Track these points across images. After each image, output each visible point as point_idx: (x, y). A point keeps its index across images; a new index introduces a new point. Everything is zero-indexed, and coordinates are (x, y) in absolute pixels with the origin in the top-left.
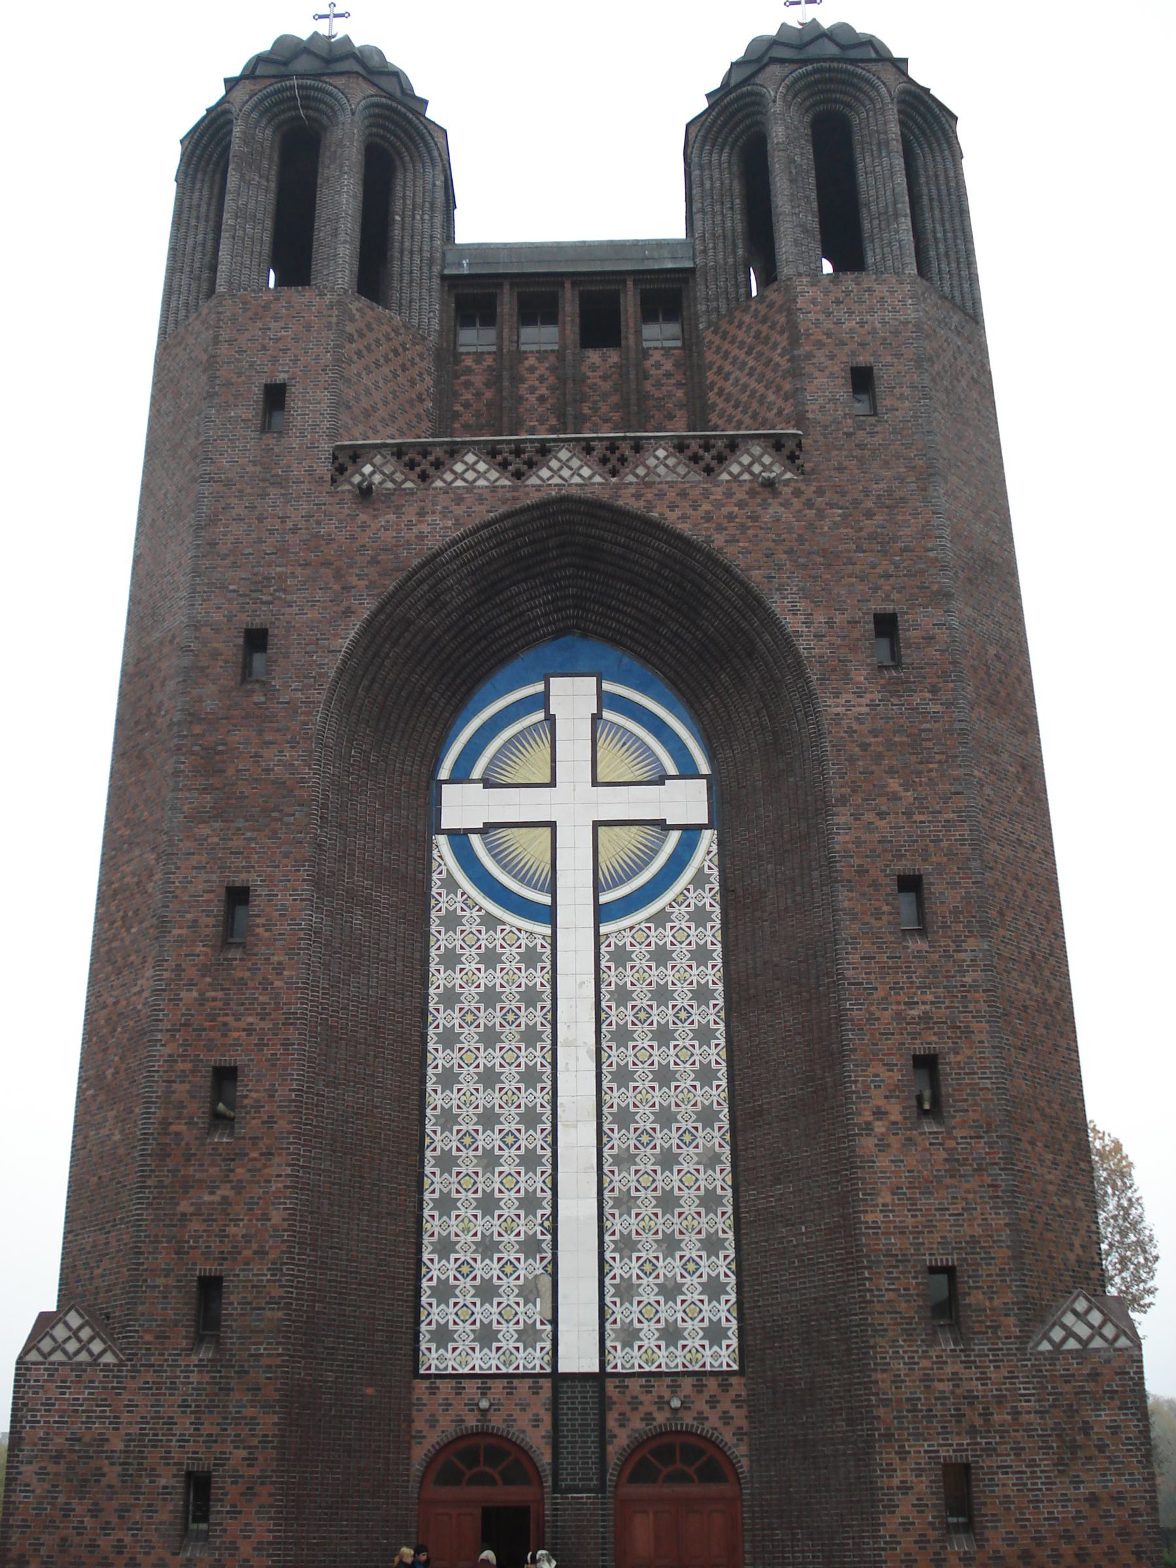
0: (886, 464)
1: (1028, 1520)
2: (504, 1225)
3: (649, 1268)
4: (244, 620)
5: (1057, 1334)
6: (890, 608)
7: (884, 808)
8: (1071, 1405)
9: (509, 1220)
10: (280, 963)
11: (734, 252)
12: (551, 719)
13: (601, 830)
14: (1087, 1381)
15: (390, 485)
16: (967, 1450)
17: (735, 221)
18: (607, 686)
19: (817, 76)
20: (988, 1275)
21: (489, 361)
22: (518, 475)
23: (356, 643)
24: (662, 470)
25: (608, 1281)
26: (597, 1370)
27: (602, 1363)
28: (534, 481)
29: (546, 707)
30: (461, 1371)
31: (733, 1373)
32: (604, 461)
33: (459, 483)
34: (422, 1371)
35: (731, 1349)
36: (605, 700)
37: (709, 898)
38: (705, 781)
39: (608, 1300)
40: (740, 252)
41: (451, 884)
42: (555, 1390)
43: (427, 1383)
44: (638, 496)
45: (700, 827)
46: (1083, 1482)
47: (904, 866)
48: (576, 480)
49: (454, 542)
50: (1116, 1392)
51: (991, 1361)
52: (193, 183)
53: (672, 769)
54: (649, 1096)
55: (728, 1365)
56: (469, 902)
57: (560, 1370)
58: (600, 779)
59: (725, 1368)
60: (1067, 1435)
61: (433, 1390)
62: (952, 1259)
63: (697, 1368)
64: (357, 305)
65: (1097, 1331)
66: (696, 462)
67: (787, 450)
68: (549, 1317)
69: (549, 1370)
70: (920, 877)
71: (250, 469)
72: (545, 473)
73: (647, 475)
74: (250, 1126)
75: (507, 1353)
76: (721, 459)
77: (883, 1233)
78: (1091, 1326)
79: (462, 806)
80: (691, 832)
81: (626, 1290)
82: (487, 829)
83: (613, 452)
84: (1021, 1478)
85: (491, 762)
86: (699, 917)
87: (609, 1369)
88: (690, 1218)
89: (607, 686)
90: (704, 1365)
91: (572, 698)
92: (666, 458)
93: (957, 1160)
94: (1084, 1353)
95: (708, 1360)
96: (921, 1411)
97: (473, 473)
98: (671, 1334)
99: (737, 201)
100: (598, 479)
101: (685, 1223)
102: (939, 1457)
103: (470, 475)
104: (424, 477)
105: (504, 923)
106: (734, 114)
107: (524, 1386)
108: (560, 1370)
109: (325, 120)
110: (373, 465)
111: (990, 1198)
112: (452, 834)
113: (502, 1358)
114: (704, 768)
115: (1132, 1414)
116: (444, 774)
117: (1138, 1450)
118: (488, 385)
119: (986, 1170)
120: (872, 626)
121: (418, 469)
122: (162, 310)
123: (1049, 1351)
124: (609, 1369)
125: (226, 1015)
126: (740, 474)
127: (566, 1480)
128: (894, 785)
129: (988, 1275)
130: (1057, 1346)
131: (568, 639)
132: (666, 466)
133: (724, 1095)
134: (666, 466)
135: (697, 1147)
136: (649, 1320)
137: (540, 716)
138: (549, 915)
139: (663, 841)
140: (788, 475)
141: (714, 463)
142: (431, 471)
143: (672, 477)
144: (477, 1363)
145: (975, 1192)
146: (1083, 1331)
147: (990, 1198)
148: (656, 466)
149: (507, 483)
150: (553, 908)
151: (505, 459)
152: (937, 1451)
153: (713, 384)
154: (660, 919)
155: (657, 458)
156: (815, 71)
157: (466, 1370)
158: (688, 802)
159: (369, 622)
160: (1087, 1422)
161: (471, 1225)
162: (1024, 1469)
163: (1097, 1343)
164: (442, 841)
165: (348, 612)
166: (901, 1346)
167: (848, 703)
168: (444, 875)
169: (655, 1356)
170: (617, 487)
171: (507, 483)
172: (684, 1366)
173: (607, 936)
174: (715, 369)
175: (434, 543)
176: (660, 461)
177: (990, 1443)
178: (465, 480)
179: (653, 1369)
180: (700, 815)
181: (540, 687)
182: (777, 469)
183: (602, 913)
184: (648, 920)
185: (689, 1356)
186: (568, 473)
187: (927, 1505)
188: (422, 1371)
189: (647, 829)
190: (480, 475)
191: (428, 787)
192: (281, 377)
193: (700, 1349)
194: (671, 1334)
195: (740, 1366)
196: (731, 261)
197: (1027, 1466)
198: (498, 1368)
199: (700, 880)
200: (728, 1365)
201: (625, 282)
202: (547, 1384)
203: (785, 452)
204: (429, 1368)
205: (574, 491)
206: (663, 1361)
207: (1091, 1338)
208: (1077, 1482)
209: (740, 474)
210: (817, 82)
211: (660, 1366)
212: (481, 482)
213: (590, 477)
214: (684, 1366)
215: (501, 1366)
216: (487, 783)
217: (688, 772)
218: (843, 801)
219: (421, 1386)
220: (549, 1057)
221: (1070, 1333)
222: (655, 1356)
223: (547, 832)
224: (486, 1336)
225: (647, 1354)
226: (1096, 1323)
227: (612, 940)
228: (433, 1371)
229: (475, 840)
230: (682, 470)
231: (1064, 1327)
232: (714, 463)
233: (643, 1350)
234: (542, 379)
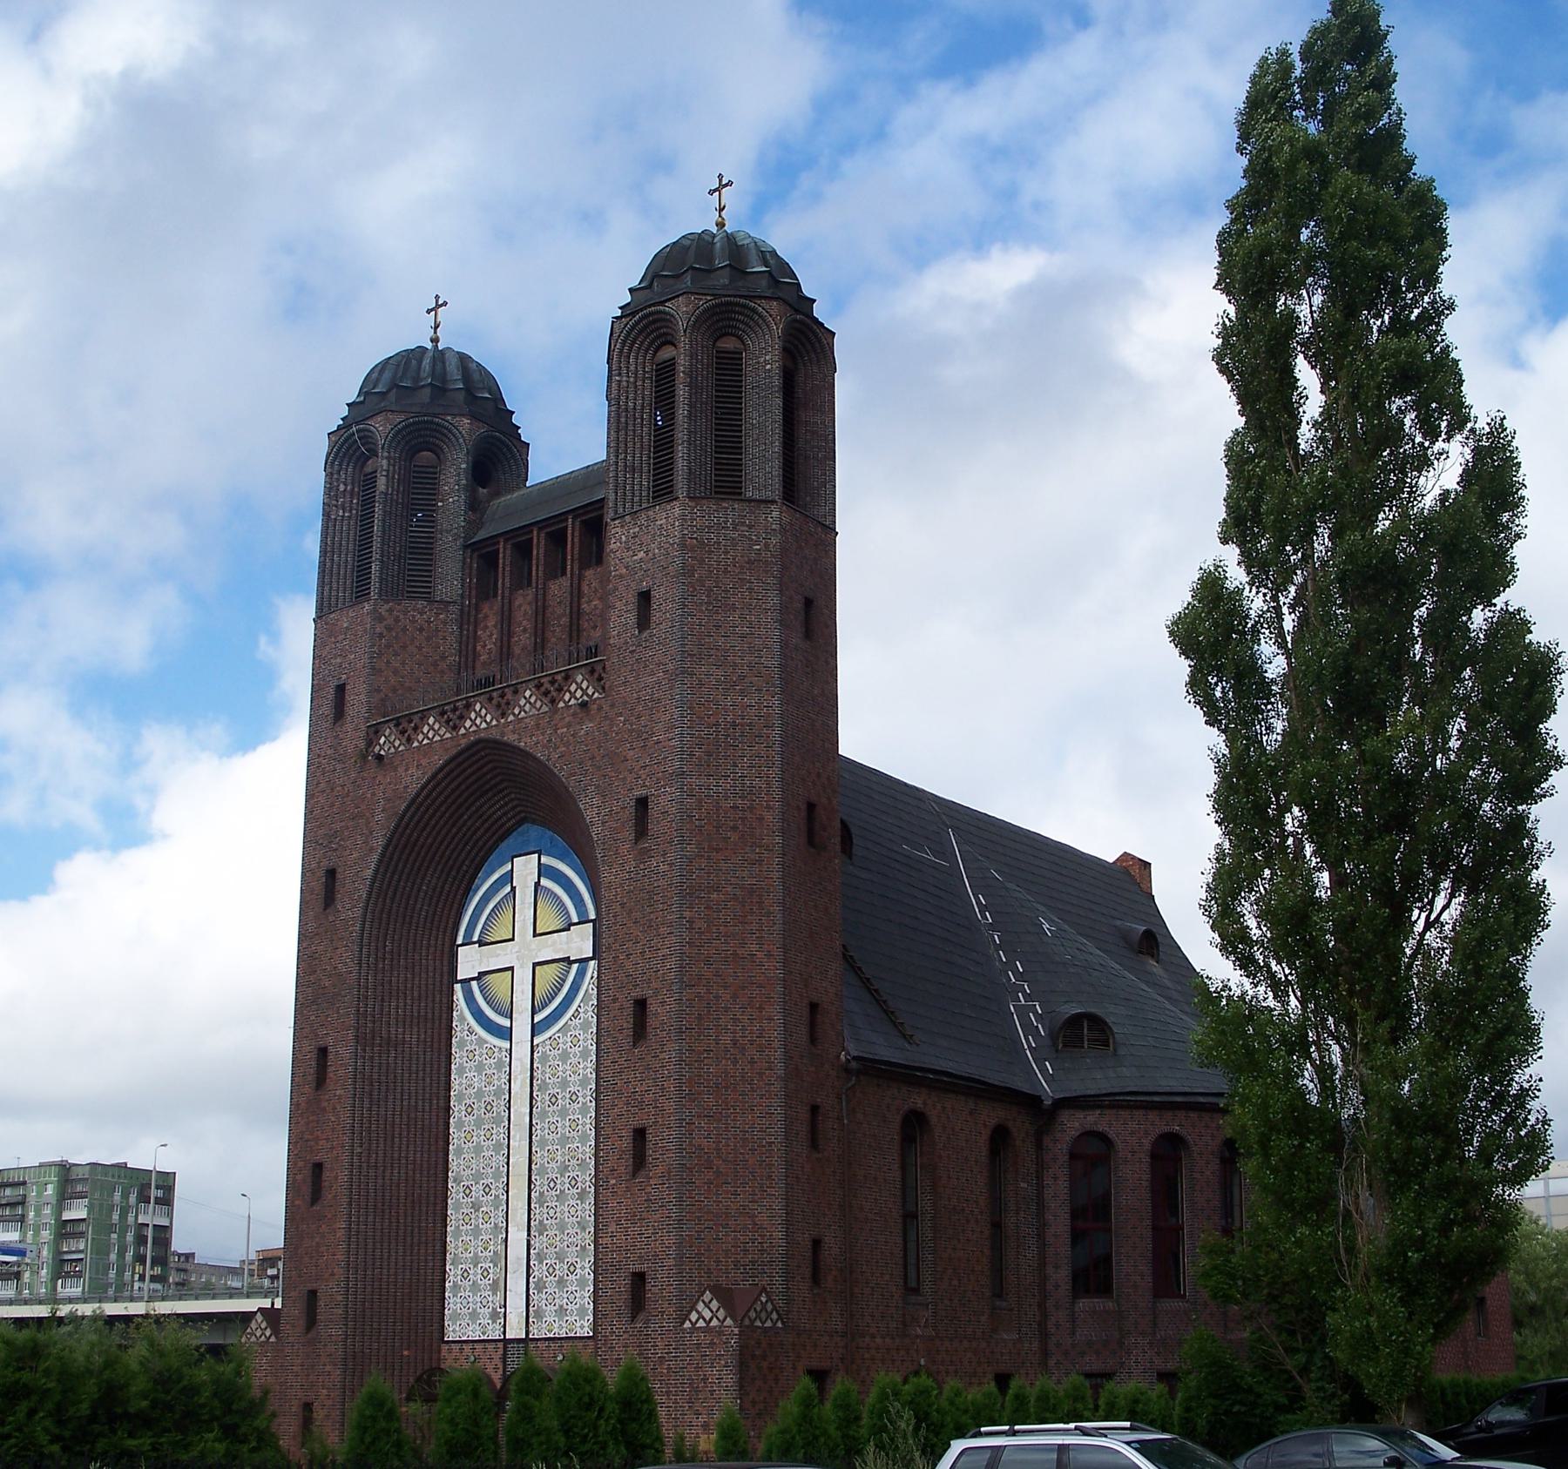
0: (652, 674)
3: (551, 1271)
5: (694, 1316)
12: (513, 889)
23: (377, 871)
27: (527, 1333)
28: (463, 731)
36: (543, 870)
41: (462, 1018)
42: (505, 1348)
44: (514, 732)
45: (587, 960)
48: (484, 725)
49: (423, 788)
61: (450, 1351)
65: (714, 1315)
67: (597, 674)
74: (328, 1196)
79: (469, 962)
81: (541, 1287)
82: (482, 974)
89: (543, 859)
91: (525, 869)
94: (708, 1329)
97: (433, 731)
98: (562, 1311)
107: (491, 1346)
116: (459, 941)
131: (525, 827)
138: (506, 1033)
146: (707, 1314)
156: (641, 320)
158: (580, 942)
159: (383, 855)
163: (715, 1322)
164: (458, 987)
165: (372, 849)
175: (414, 789)
176: (528, 703)
183: (535, 1030)
186: (480, 720)
189: (560, 965)
202: (500, 1345)
210: (646, 327)
219: (445, 1347)
221: (701, 1317)
225: (550, 1326)
230: (539, 704)
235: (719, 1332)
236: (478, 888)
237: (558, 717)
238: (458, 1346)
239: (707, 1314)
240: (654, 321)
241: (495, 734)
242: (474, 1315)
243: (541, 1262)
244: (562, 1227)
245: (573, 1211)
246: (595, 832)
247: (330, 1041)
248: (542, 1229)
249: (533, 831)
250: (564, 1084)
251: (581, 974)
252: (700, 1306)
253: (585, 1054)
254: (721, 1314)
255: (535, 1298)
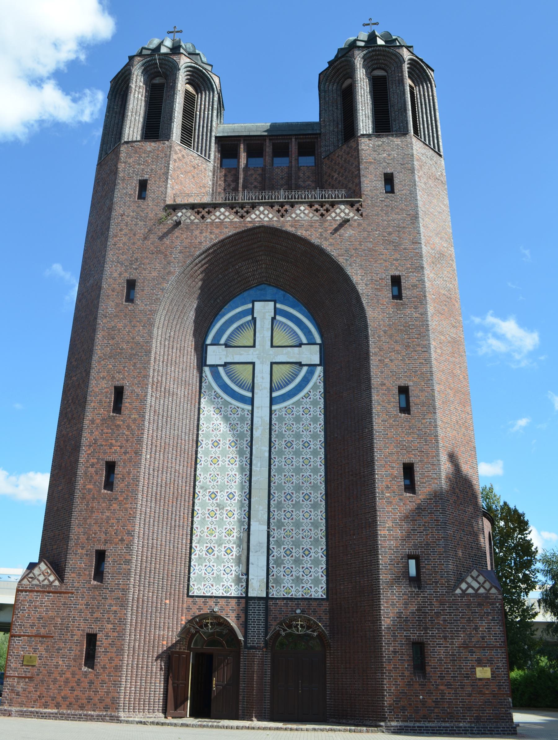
1: (450, 668)
2: (227, 532)
3: (288, 553)
4: (127, 276)
5: (464, 586)
6: (397, 273)
7: (393, 358)
8: (470, 618)
9: (230, 530)
10: (135, 418)
11: (338, 127)
12: (254, 319)
13: (274, 366)
14: (477, 607)
15: (189, 221)
16: (423, 636)
17: (338, 114)
18: (278, 306)
19: (374, 53)
20: (434, 559)
21: (233, 172)
22: (242, 217)
24: (302, 215)
25: (271, 557)
26: (264, 595)
27: (267, 593)
28: (249, 219)
29: (253, 314)
30: (207, 595)
31: (323, 599)
32: (279, 211)
33: (217, 220)
34: (190, 594)
35: (323, 589)
36: (276, 311)
37: (318, 396)
38: (318, 346)
39: (271, 566)
40: (340, 126)
42: (247, 603)
43: (191, 600)
44: (292, 226)
45: (315, 365)
46: (474, 652)
47: (402, 383)
48: (266, 219)
50: (490, 613)
51: (434, 597)
52: (115, 99)
53: (305, 341)
54: (291, 479)
55: (322, 596)
56: (217, 395)
57: (249, 596)
58: (274, 344)
59: (320, 597)
60: (468, 631)
62: (418, 552)
63: (308, 597)
64: (179, 148)
65: (482, 586)
66: (317, 212)
68: (245, 571)
69: (244, 595)
70: (408, 387)
71: (132, 214)
72: (253, 216)
73: (296, 217)
75: (227, 587)
76: (327, 210)
77: (388, 540)
78: (479, 583)
80: (312, 366)
81: (279, 562)
82: (226, 365)
83: (282, 208)
84: (447, 650)
85: (229, 337)
86: (315, 403)
87: (270, 596)
88: (307, 531)
89: (278, 306)
90: (311, 595)
91: (264, 310)
92: (304, 210)
93: (421, 509)
94: (476, 594)
95: (313, 593)
96: (403, 618)
98: (298, 580)
99: (339, 106)
100: (275, 219)
101: (304, 534)
102: (411, 639)
103: (222, 217)
104: (203, 217)
105: (231, 404)
106: (338, 70)
108: (249, 596)
109: (168, 73)
110: (182, 213)
111: (435, 525)
112: (211, 366)
113: (225, 589)
114: (319, 340)
115: (497, 623)
116: (209, 341)
117: (500, 639)
118: (233, 181)
119: (434, 513)
120: (390, 281)
121: (201, 215)
122: (100, 150)
123: (460, 594)
124: (270, 596)
125: (112, 440)
126: (335, 217)
127: (250, 643)
128: (398, 348)
129: (434, 559)
130: (464, 591)
131: (263, 286)
132: (304, 213)
133: (323, 479)
134: (304, 213)
135: (311, 501)
136: (288, 575)
137: (249, 318)
138: (251, 401)
139: (300, 371)
140: (356, 217)
141: (324, 212)
142: (206, 215)
143: (307, 218)
144: (214, 591)
145: (429, 523)
146: (476, 585)
147: (435, 525)
148: (300, 213)
149: (238, 220)
150: (252, 399)
151: (237, 211)
152: (410, 636)
153: (327, 181)
154: (298, 403)
155: (300, 210)
157: (209, 594)
158: (311, 355)
160: (477, 626)
161: (213, 532)
162: (448, 645)
163: (482, 591)
164: (207, 370)
166: (395, 589)
167: (378, 312)
168: (207, 384)
169: (290, 591)
170: (283, 222)
171: (238, 220)
172: (303, 595)
173: (275, 411)
174: (328, 174)
177: (433, 633)
178: (220, 219)
179: (289, 596)
180: (316, 360)
181: (250, 306)
182: (351, 215)
183: (272, 401)
184: (293, 404)
185: (305, 591)
186: (263, 216)
187: (405, 660)
188: (190, 594)
189: (293, 366)
190: (226, 217)
191: (202, 347)
192: (146, 177)
193: (310, 588)
194: (298, 580)
195: (327, 596)
196: (336, 130)
197: (450, 644)
198: (223, 594)
199: (315, 387)
200: (322, 596)
201: (291, 139)
202: (243, 601)
203: (355, 207)
204: (193, 593)
205: (266, 224)
206: (293, 593)
207: (479, 588)
208: (472, 652)
209: (335, 217)
210: (373, 56)
211: (292, 595)
212: (227, 220)
213: (272, 218)
214: (303, 595)
215: (224, 593)
216: (227, 345)
217: (312, 343)
218: (376, 354)
220: (249, 461)
221: (470, 586)
222: (290, 591)
223: (251, 366)
224: (218, 579)
225: (287, 588)
226: (481, 582)
227: (277, 412)
228: (195, 594)
229: (221, 369)
230: (311, 215)
231: (467, 583)
232: (324, 212)
233: (285, 588)
234: (256, 179)
235: (487, 596)
236: (224, 315)
237: (327, 224)
238: (203, 599)
239: (476, 585)
240: (377, 55)
241: (276, 225)
242: (218, 579)
243: (279, 546)
244: (298, 525)
245: (307, 515)
246: (361, 288)
247: (126, 383)
248: (280, 525)
249: (271, 291)
250: (298, 436)
251: (310, 374)
252: (469, 579)
253: (315, 420)
254: (487, 585)
255: (274, 571)
